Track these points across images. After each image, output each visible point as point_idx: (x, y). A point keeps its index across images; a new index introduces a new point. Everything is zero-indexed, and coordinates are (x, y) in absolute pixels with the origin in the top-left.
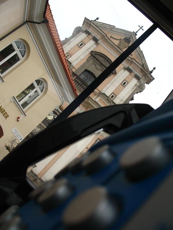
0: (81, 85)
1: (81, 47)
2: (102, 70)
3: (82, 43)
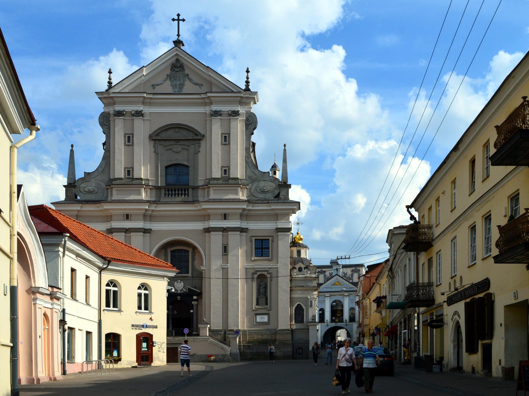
0: (178, 194)
2: (184, 147)
3: (127, 136)
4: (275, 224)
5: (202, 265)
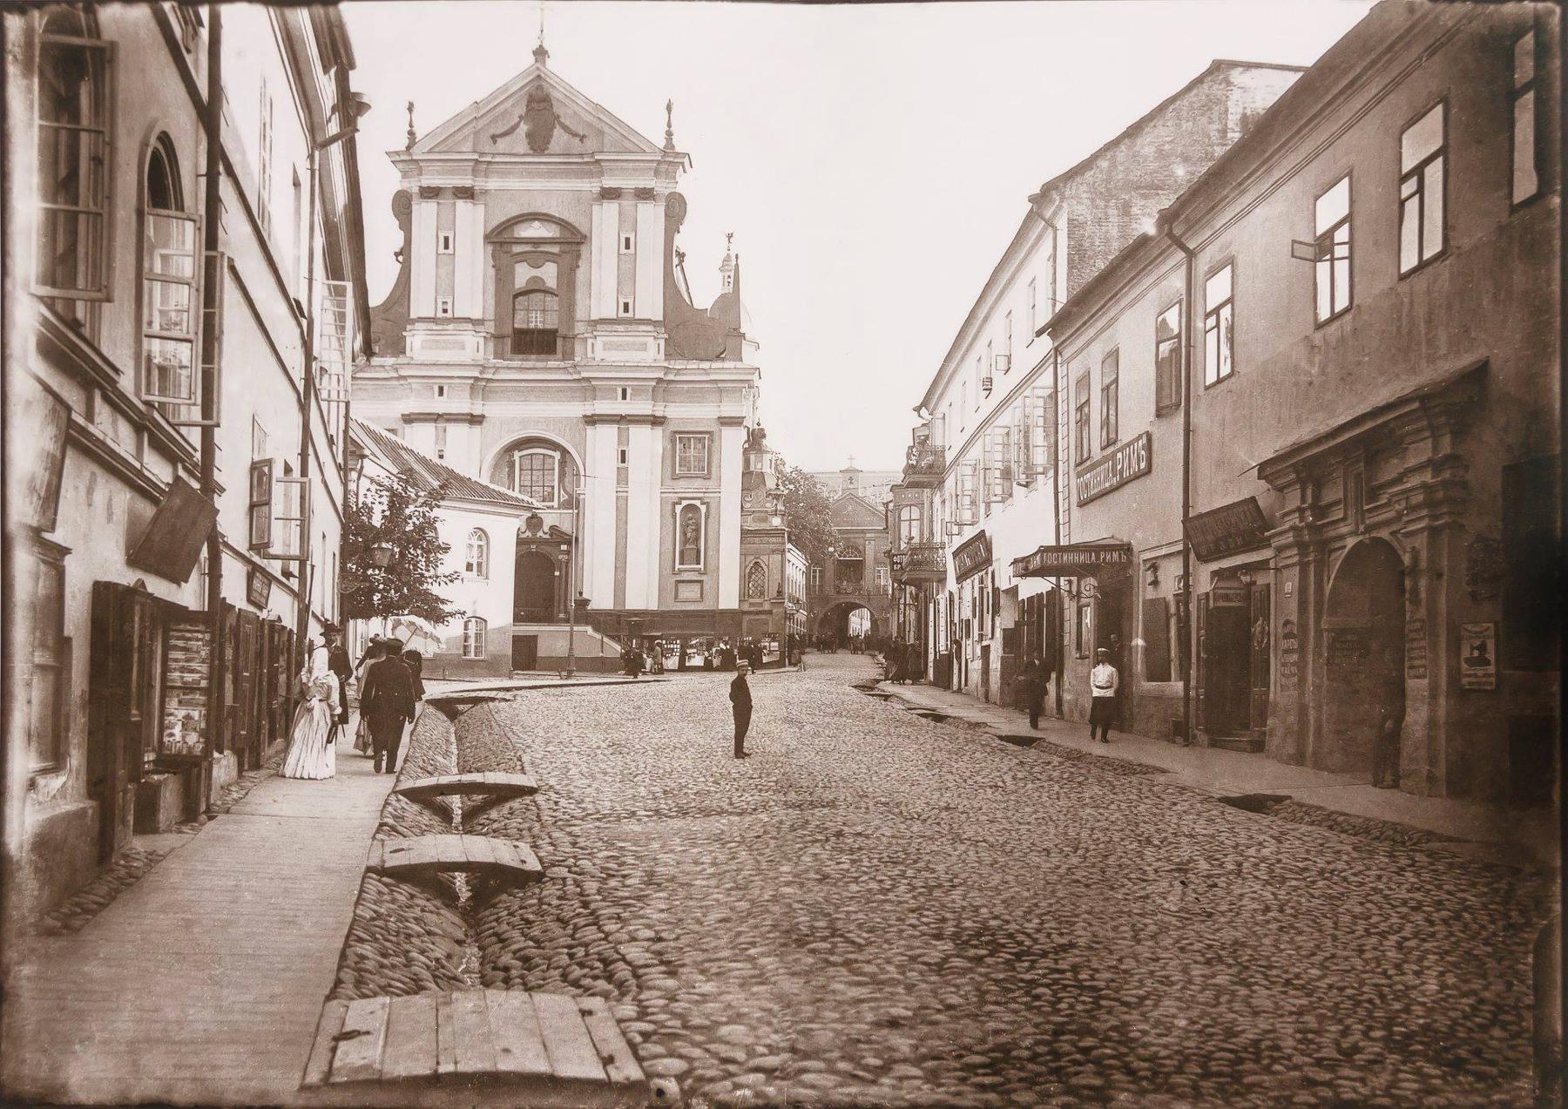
5: (578, 486)
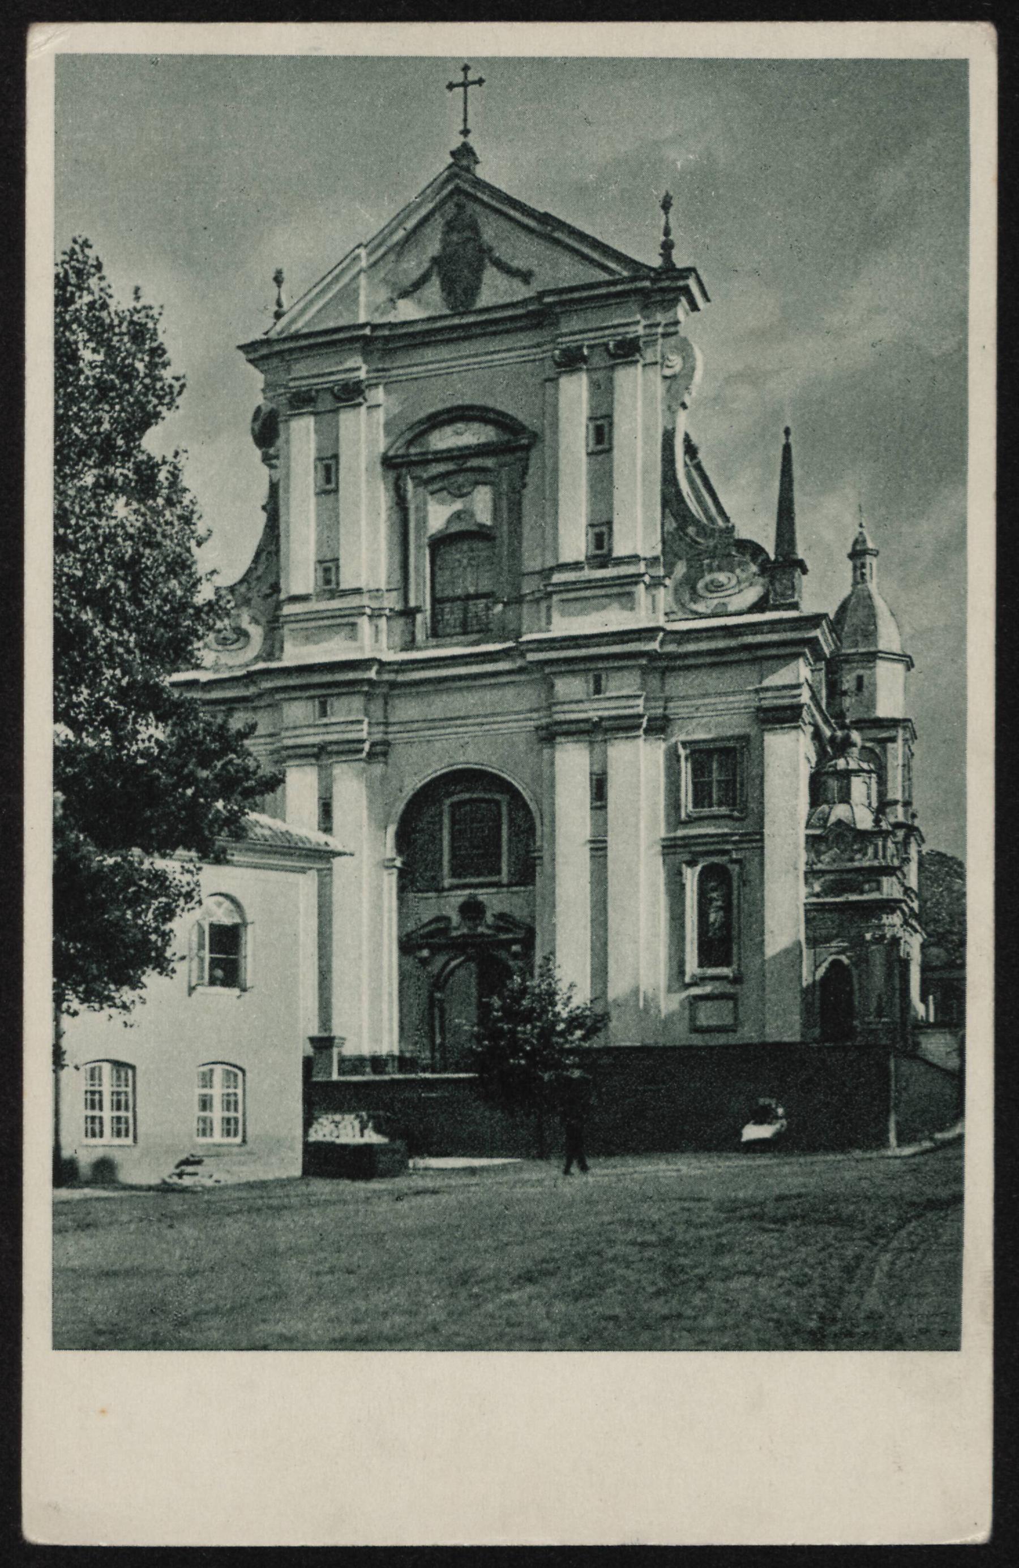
1: (333, 486)
4: (753, 696)
